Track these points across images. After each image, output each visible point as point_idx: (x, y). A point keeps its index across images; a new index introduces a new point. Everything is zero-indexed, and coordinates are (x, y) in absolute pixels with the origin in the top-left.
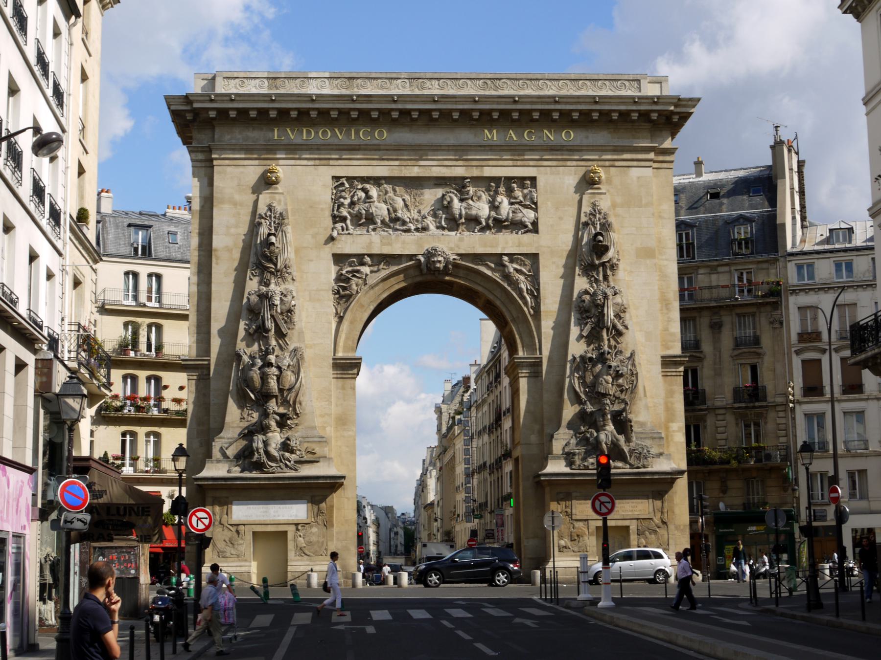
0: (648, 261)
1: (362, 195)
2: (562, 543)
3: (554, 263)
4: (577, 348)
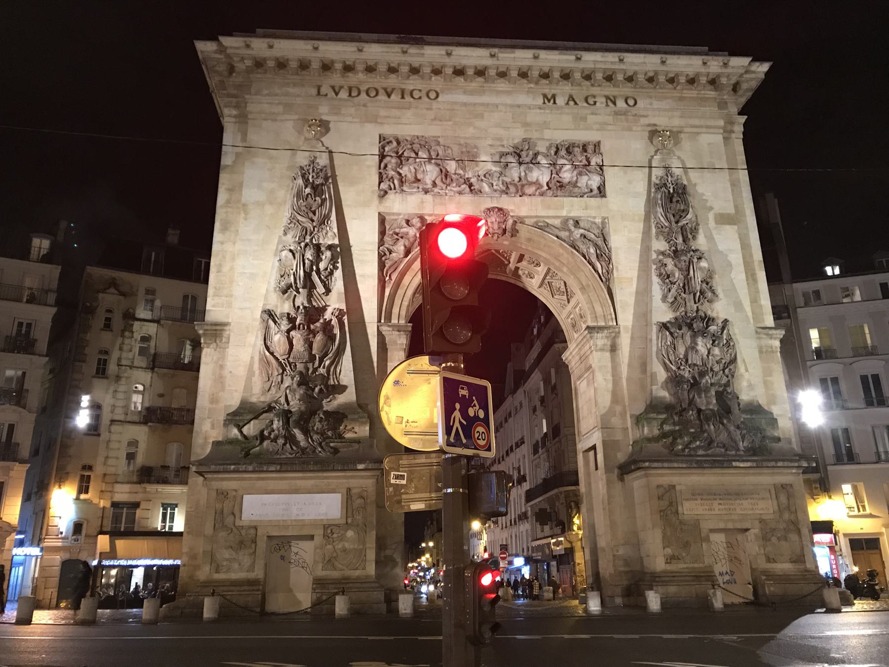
0: (728, 227)
1: (413, 155)
2: (669, 551)
3: (625, 227)
4: (663, 313)
